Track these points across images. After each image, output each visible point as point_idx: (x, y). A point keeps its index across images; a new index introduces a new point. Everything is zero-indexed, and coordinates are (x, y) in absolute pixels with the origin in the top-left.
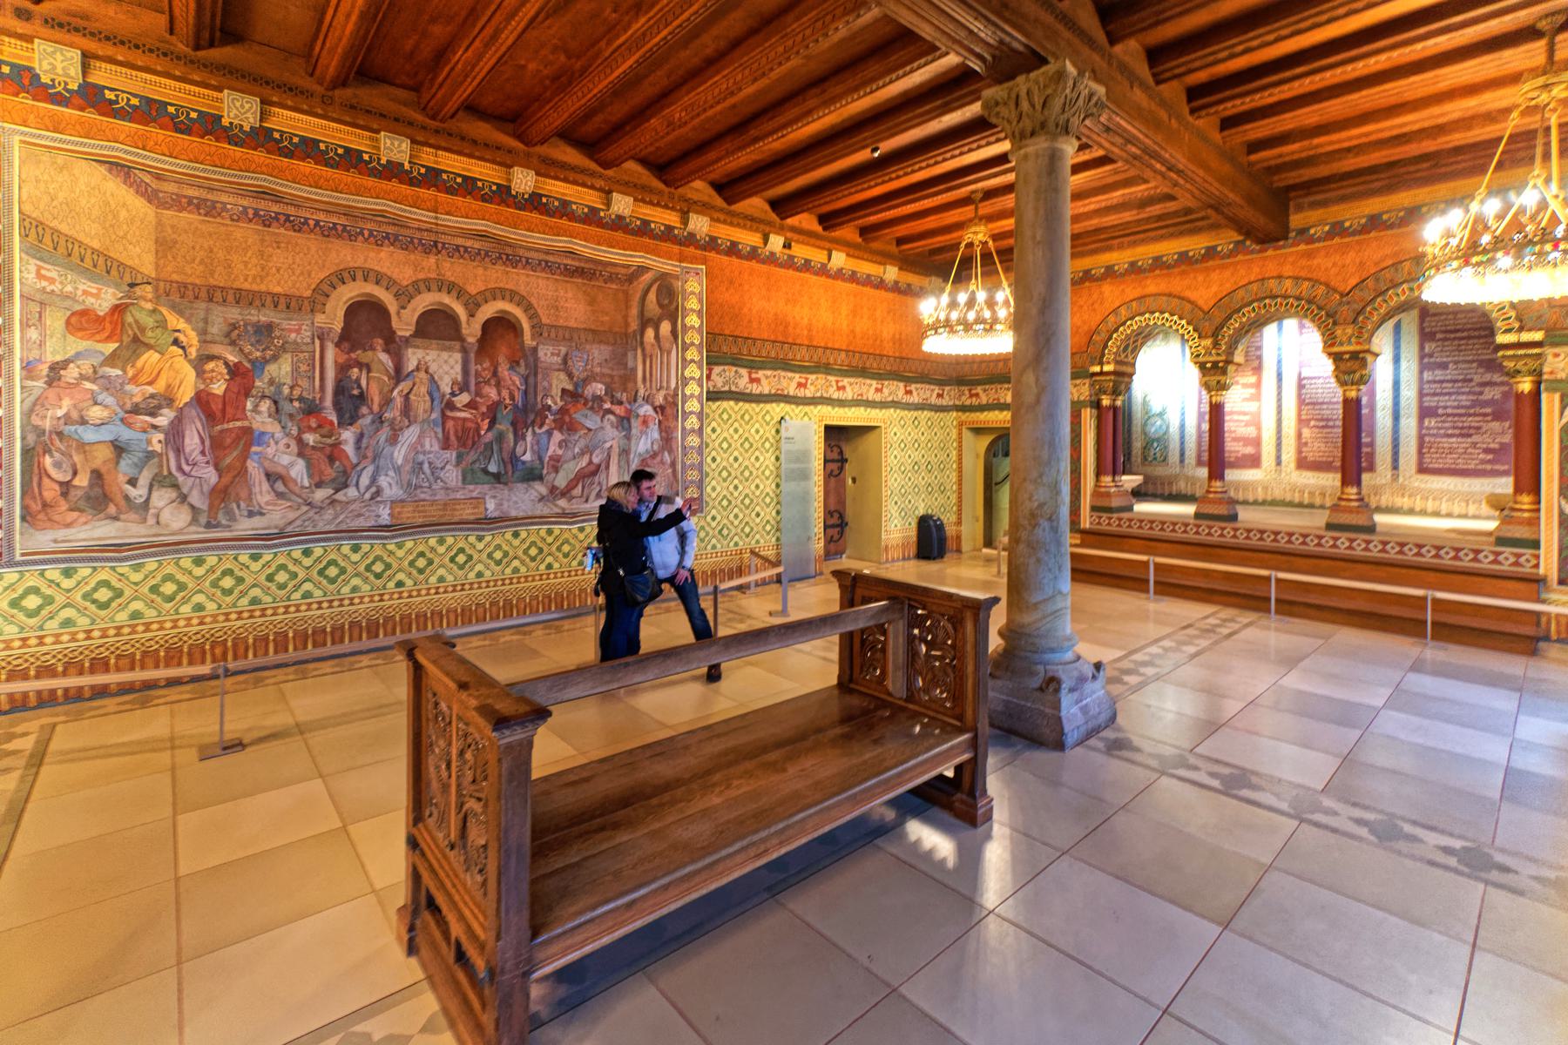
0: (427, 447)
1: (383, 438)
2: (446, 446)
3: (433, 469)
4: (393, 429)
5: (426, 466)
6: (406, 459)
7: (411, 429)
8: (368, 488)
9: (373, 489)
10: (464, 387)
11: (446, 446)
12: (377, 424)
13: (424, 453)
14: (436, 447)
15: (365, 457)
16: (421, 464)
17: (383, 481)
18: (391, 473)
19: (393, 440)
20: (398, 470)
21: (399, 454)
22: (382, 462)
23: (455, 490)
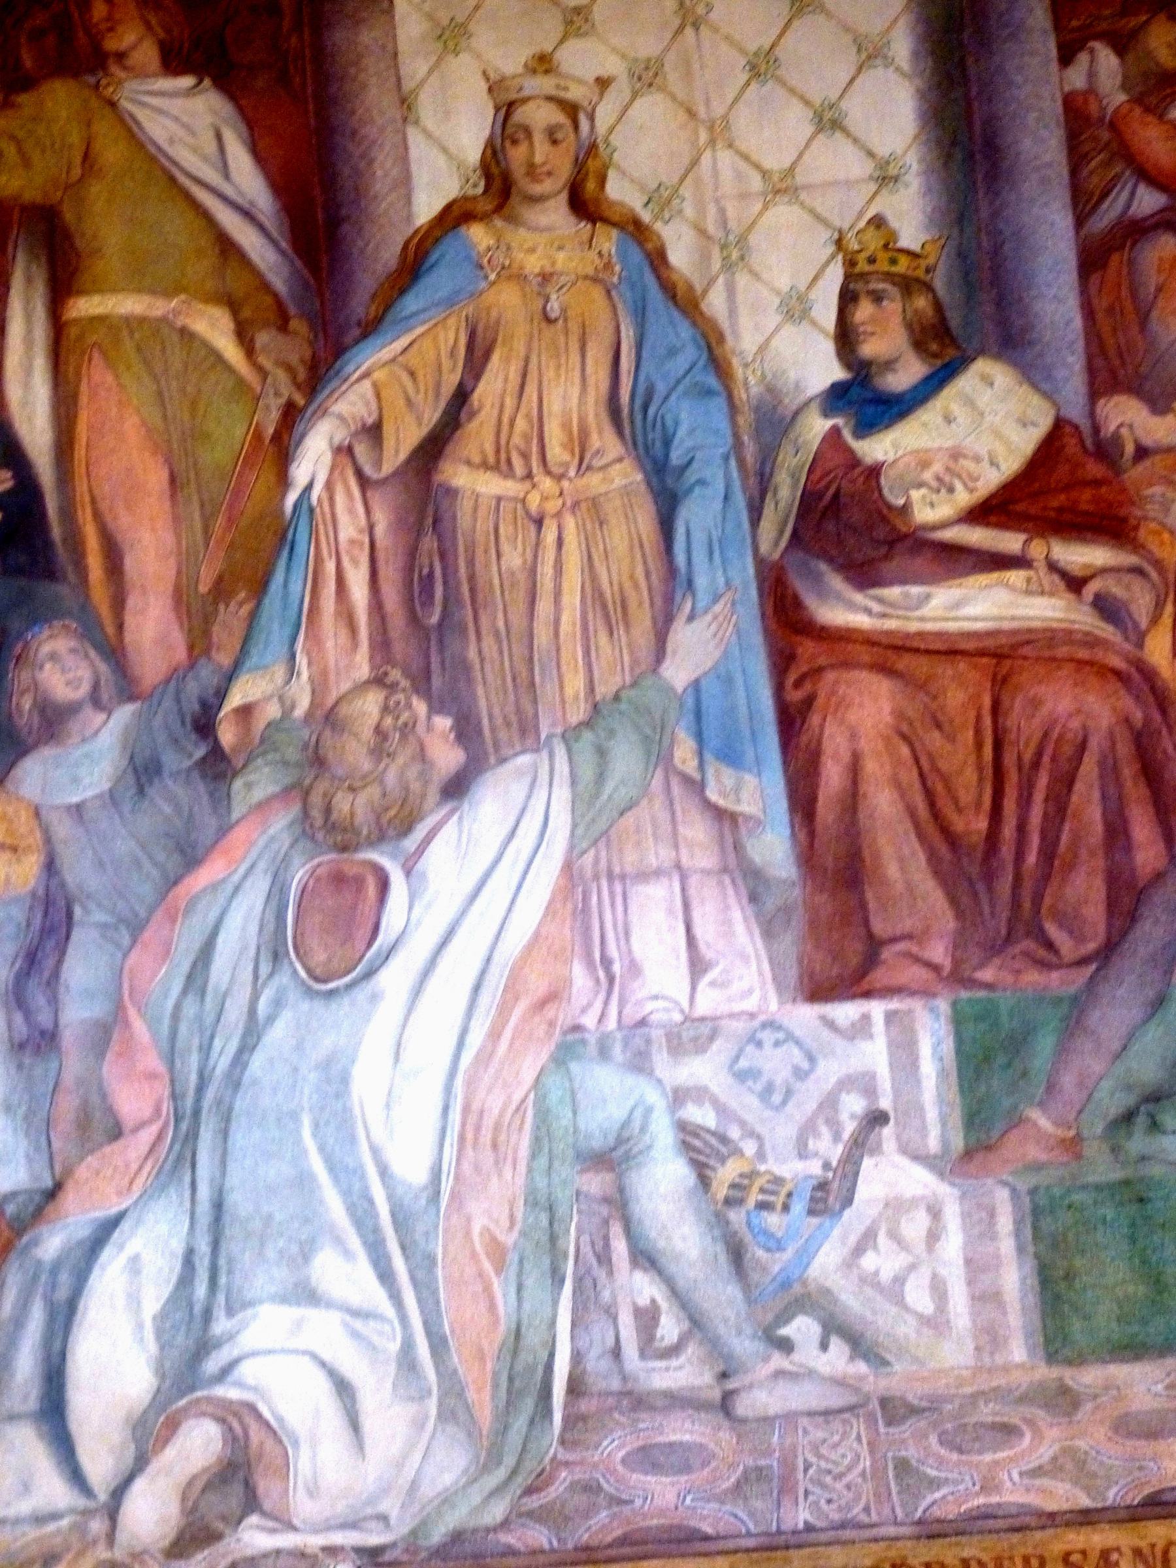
0: (661, 980)
1: (242, 924)
2: (842, 958)
3: (732, 1201)
4: (331, 832)
5: (662, 1184)
6: (469, 1130)
7: (493, 803)
8: (151, 1432)
9: (198, 1444)
10: (959, 311)
11: (842, 958)
12: (178, 792)
13: (637, 1046)
14: (747, 974)
15: (101, 1127)
16: (613, 1158)
17: (278, 1360)
18: (345, 1274)
19: (335, 928)
20: (400, 1238)
21: (402, 1062)
22: (252, 1168)
23: (973, 1424)
